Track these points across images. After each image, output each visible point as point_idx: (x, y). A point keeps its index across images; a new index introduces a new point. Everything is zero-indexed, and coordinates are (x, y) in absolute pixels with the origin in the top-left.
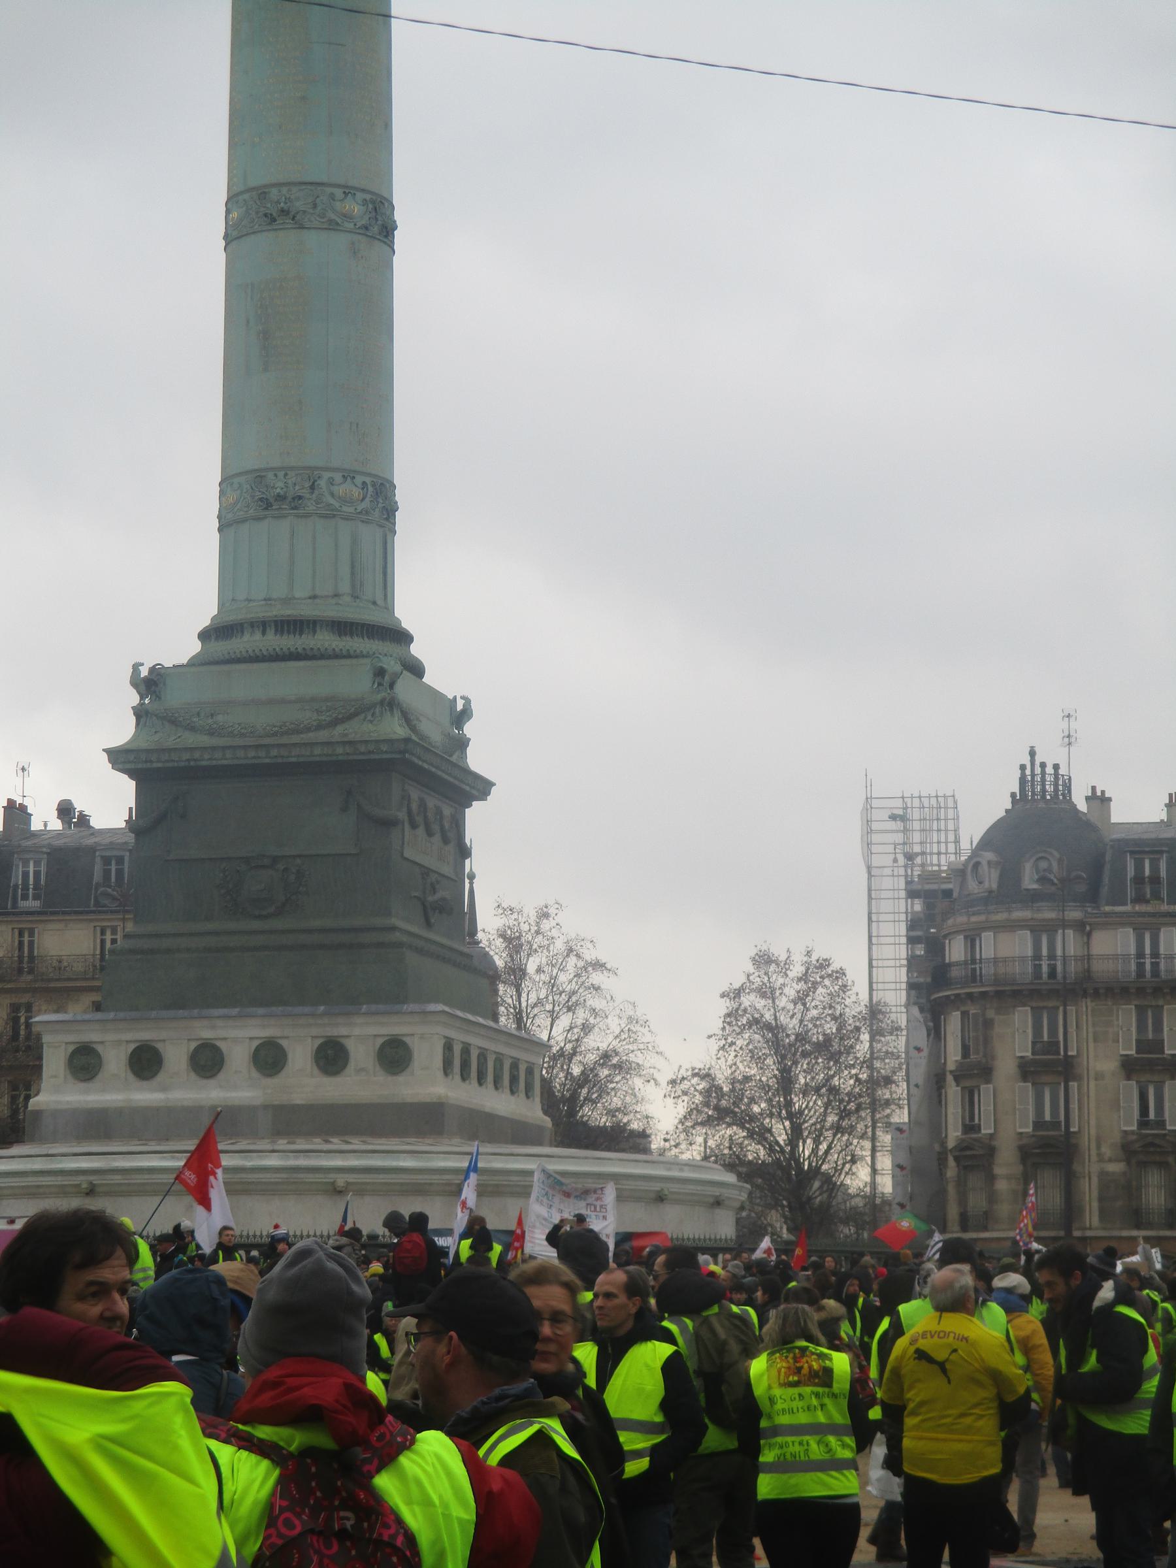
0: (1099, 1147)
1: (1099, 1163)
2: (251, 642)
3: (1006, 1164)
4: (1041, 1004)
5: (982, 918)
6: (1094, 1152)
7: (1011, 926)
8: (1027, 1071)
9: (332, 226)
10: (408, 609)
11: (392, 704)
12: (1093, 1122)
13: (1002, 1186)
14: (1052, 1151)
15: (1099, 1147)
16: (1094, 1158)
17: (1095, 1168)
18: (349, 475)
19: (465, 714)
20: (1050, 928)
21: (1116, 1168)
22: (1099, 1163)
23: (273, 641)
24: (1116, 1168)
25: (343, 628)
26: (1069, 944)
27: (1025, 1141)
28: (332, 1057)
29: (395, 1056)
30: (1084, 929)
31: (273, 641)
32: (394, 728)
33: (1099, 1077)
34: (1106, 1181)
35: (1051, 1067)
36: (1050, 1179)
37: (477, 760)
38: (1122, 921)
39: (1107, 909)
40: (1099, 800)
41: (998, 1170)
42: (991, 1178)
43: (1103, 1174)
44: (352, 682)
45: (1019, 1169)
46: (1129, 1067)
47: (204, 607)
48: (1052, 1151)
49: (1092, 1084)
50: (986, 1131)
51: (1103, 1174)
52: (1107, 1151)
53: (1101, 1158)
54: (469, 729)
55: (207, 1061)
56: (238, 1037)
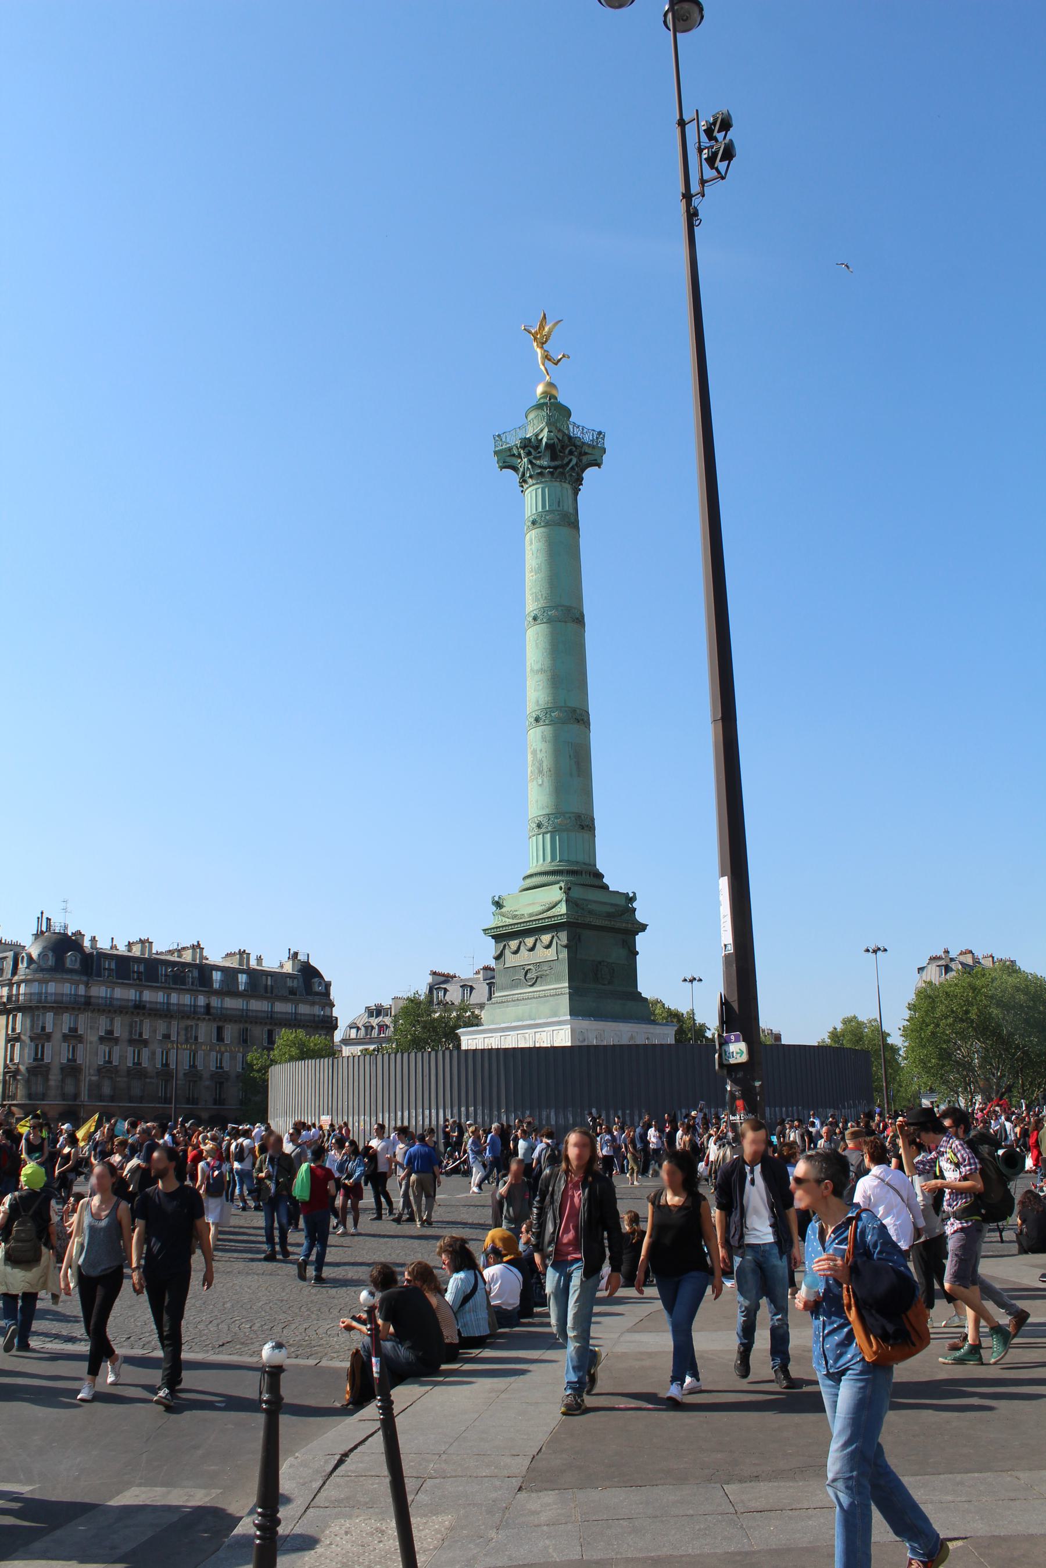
1: (88, 1077)
8: (65, 1037)
10: (601, 867)
13: (52, 1083)
14: (72, 1070)
21: (94, 1078)
22: (88, 1077)
26: (82, 990)
33: (91, 1043)
36: (69, 1081)
41: (50, 1077)
42: (47, 1080)
43: (90, 1080)
45: (60, 1077)
46: (102, 1039)
48: (72, 1070)
51: (90, 1080)
52: (92, 1071)
53: (90, 1075)
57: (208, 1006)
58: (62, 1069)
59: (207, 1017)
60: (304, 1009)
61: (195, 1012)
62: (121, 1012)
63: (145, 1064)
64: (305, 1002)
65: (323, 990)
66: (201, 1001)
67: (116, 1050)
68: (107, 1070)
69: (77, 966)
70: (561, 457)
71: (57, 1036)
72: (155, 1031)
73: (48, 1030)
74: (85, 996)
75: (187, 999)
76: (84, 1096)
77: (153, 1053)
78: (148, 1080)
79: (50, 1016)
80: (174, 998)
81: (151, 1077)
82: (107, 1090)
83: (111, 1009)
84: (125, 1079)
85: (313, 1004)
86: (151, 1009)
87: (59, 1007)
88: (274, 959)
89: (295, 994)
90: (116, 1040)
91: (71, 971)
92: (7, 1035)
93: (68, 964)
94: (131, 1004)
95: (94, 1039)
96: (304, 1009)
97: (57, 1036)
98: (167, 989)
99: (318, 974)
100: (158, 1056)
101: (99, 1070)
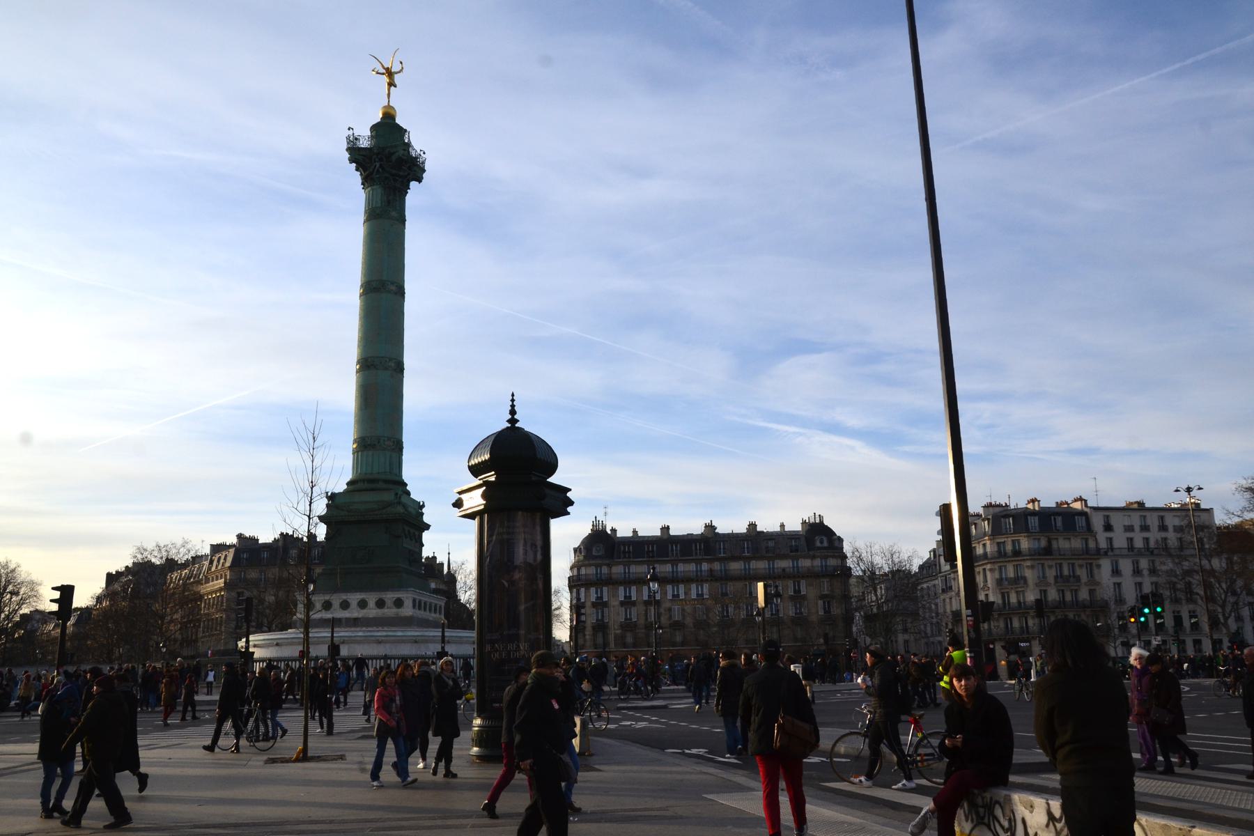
2: (360, 486)
3: (589, 631)
8: (594, 605)
9: (386, 369)
10: (406, 476)
11: (399, 503)
14: (601, 627)
18: (389, 439)
19: (423, 506)
20: (600, 566)
23: (366, 485)
25: (386, 481)
26: (605, 570)
28: (380, 604)
29: (399, 603)
30: (609, 566)
31: (366, 485)
32: (400, 509)
34: (616, 635)
37: (426, 519)
38: (620, 563)
40: (614, 531)
44: (388, 497)
46: (622, 604)
47: (349, 476)
54: (424, 510)
55: (327, 606)
56: (354, 598)
57: (711, 570)
60: (805, 563)
64: (805, 557)
65: (826, 544)
67: (634, 610)
68: (628, 626)
70: (387, 164)
71: (588, 604)
75: (692, 567)
76: (612, 645)
80: (681, 567)
82: (629, 640)
85: (813, 557)
88: (794, 525)
89: (797, 551)
90: (634, 604)
91: (596, 557)
95: (617, 603)
96: (805, 563)
97: (588, 604)
98: (674, 563)
99: (829, 532)
101: (622, 626)
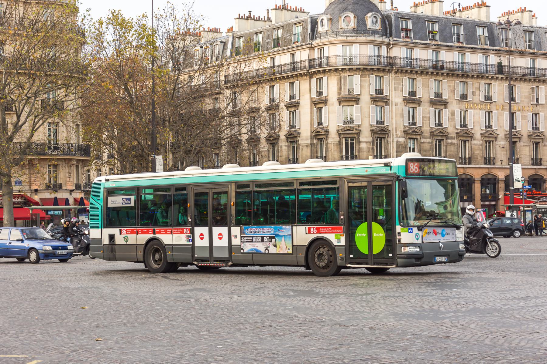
0: (396, 132)
4: (378, 75)
5: (354, 38)
6: (395, 134)
7: (367, 43)
12: (394, 122)
15: (396, 132)
16: (395, 136)
17: (395, 140)
21: (402, 140)
24: (402, 140)
26: (384, 51)
27: (373, 128)
30: (388, 45)
33: (396, 104)
35: (380, 99)
39: (395, 39)
43: (397, 141)
49: (394, 107)
50: (356, 123)
52: (399, 133)
58: (372, 131)
59: (500, 76)
61: (487, 71)
62: (422, 73)
63: (446, 124)
66: (493, 60)
69: (378, 27)
72: (453, 91)
73: (356, 92)
74: (387, 57)
77: (453, 114)
78: (449, 141)
79: (356, 78)
81: (452, 138)
83: (411, 70)
84: (429, 140)
86: (450, 70)
87: (365, 70)
92: (311, 98)
93: (369, 25)
94: (430, 64)
95: (400, 100)
100: (457, 117)
